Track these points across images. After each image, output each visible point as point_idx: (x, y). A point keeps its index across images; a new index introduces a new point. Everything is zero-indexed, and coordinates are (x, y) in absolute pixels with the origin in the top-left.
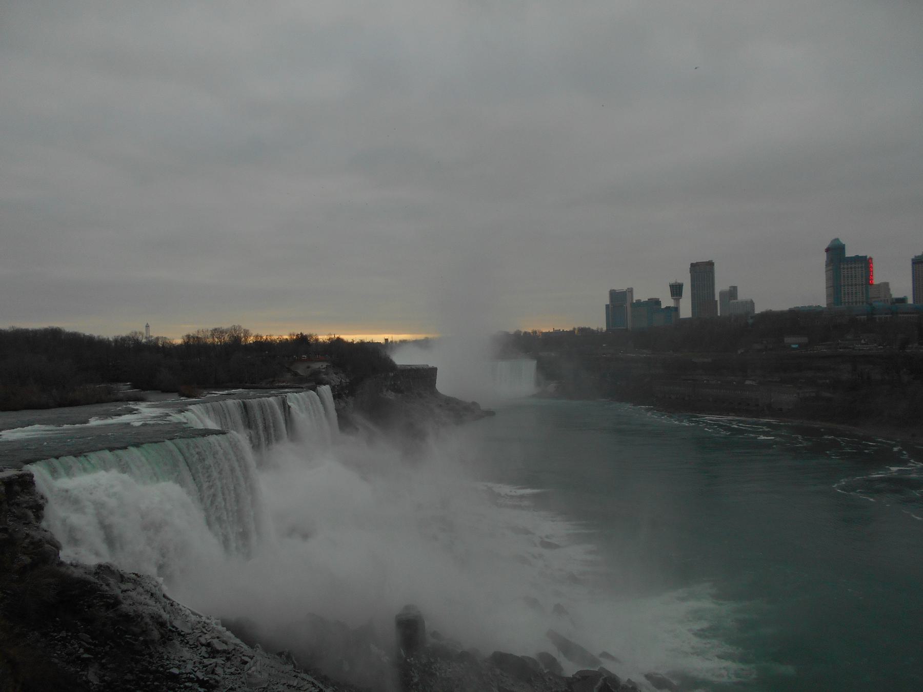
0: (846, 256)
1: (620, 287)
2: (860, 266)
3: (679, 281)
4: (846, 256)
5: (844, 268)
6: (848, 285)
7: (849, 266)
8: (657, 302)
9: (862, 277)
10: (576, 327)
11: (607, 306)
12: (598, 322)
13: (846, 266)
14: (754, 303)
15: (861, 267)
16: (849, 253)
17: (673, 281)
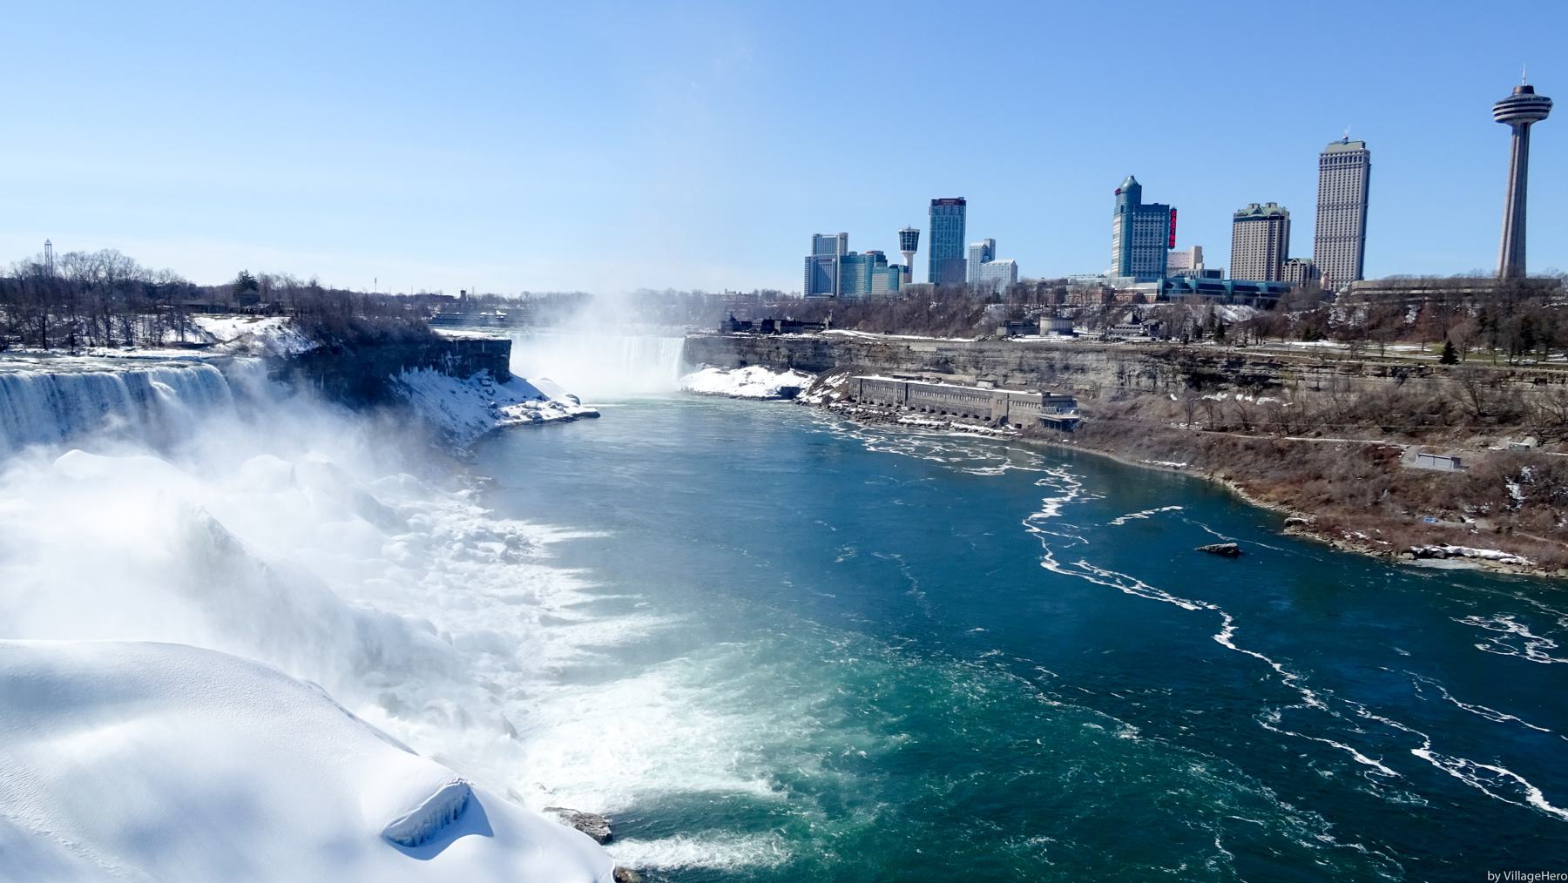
0: (1142, 203)
1: (830, 231)
2: (1159, 219)
3: (914, 227)
4: (1142, 203)
5: (1137, 222)
6: (1141, 247)
7: (1145, 218)
8: (880, 258)
9: (1160, 235)
10: (760, 290)
11: (808, 260)
12: (794, 284)
13: (1140, 218)
14: (1017, 267)
15: (1161, 221)
16: (1147, 199)
17: (904, 228)
